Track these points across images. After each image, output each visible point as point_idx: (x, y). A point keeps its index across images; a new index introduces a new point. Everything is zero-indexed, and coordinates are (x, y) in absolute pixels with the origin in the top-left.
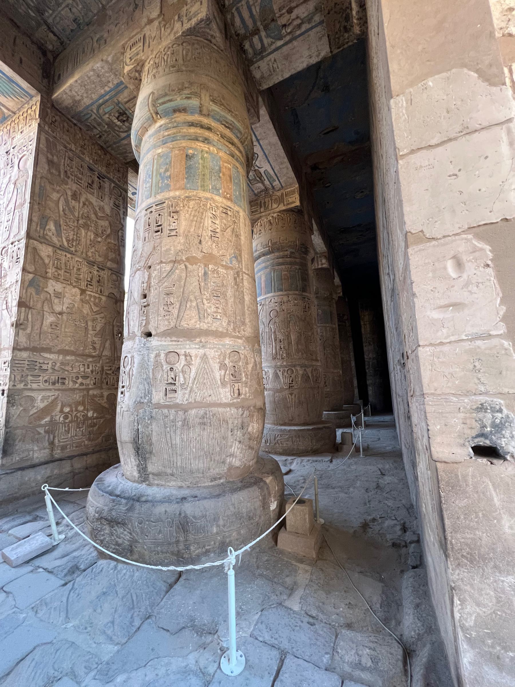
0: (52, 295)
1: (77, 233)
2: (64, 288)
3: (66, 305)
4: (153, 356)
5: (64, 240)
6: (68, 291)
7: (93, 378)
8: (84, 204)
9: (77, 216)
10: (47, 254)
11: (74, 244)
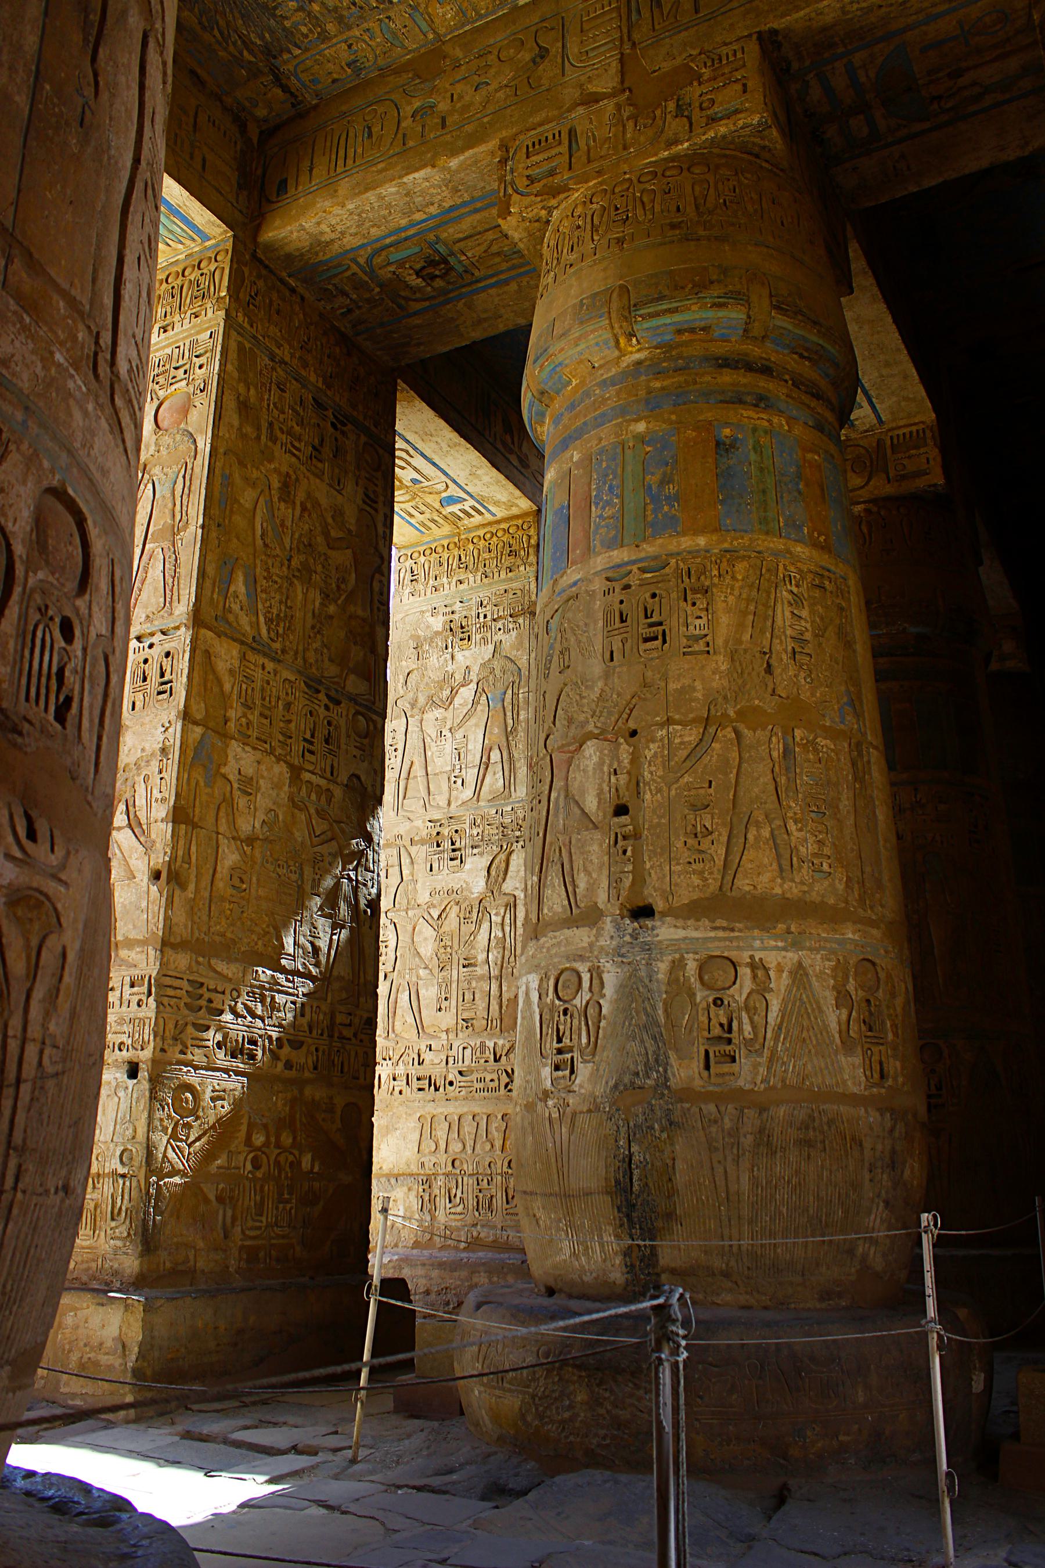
0: (236, 785)
1: (287, 598)
2: (259, 762)
3: (261, 816)
4: (662, 967)
5: (262, 619)
6: (265, 774)
7: (313, 1049)
8: (304, 509)
9: (288, 548)
10: (228, 666)
11: (281, 631)
